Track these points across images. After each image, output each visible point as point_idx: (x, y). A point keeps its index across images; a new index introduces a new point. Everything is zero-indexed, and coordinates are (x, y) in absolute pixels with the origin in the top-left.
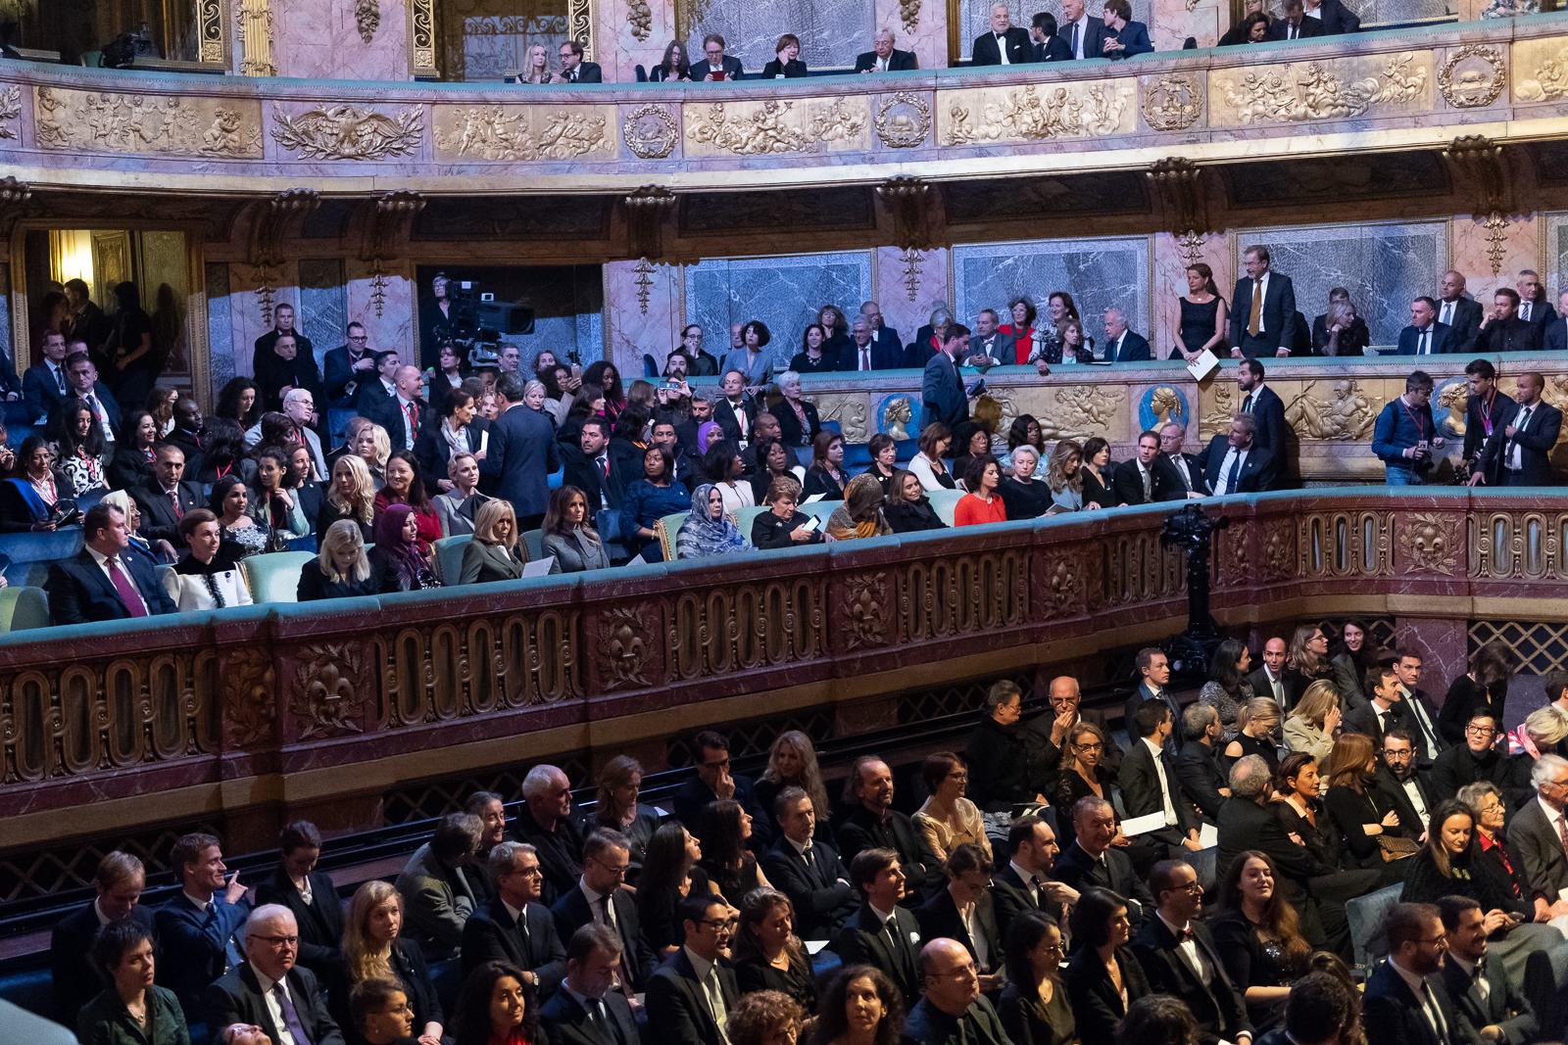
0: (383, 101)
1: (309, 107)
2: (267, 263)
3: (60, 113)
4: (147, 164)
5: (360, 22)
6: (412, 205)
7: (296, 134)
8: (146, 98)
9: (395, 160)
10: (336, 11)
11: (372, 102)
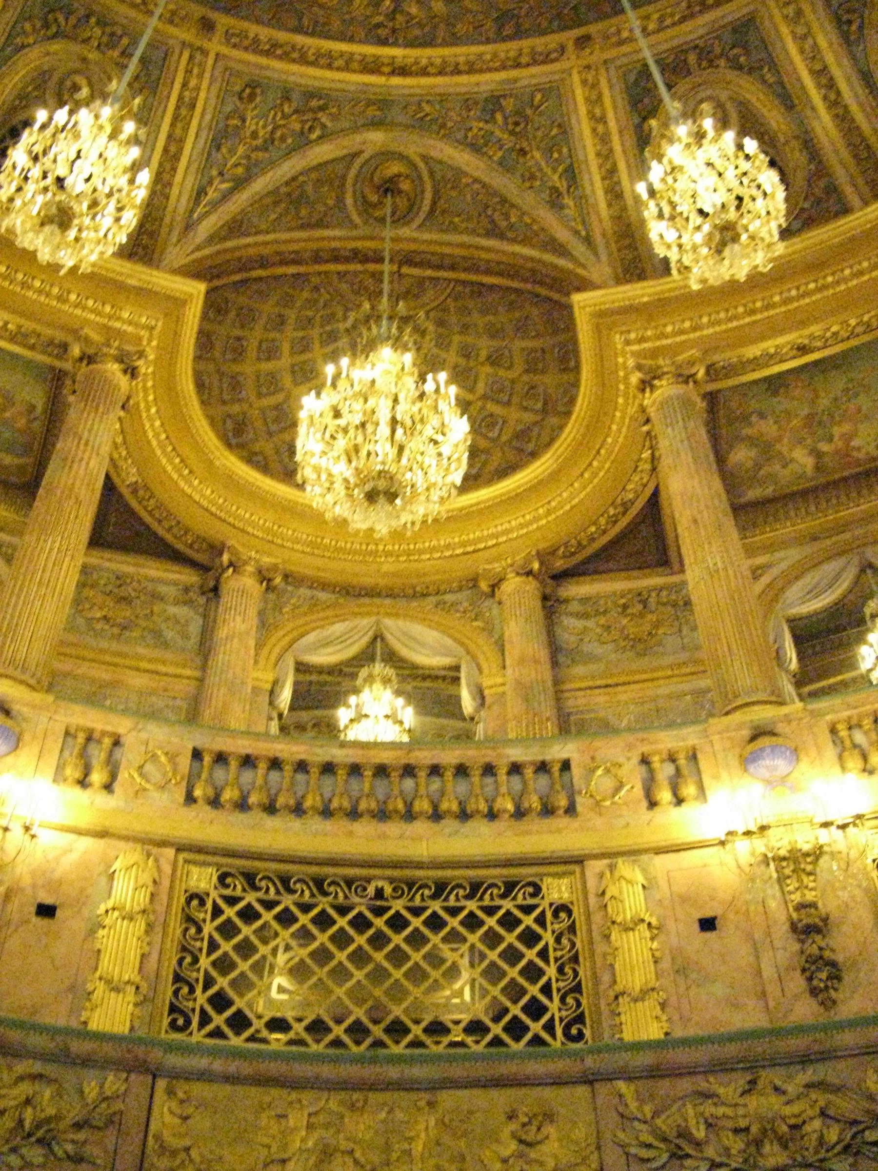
0: (826, 1056)
1: (685, 1085)
3: (201, 1123)
5: (810, 979)
7: (665, 1140)
8: (371, 1095)
11: (805, 1060)
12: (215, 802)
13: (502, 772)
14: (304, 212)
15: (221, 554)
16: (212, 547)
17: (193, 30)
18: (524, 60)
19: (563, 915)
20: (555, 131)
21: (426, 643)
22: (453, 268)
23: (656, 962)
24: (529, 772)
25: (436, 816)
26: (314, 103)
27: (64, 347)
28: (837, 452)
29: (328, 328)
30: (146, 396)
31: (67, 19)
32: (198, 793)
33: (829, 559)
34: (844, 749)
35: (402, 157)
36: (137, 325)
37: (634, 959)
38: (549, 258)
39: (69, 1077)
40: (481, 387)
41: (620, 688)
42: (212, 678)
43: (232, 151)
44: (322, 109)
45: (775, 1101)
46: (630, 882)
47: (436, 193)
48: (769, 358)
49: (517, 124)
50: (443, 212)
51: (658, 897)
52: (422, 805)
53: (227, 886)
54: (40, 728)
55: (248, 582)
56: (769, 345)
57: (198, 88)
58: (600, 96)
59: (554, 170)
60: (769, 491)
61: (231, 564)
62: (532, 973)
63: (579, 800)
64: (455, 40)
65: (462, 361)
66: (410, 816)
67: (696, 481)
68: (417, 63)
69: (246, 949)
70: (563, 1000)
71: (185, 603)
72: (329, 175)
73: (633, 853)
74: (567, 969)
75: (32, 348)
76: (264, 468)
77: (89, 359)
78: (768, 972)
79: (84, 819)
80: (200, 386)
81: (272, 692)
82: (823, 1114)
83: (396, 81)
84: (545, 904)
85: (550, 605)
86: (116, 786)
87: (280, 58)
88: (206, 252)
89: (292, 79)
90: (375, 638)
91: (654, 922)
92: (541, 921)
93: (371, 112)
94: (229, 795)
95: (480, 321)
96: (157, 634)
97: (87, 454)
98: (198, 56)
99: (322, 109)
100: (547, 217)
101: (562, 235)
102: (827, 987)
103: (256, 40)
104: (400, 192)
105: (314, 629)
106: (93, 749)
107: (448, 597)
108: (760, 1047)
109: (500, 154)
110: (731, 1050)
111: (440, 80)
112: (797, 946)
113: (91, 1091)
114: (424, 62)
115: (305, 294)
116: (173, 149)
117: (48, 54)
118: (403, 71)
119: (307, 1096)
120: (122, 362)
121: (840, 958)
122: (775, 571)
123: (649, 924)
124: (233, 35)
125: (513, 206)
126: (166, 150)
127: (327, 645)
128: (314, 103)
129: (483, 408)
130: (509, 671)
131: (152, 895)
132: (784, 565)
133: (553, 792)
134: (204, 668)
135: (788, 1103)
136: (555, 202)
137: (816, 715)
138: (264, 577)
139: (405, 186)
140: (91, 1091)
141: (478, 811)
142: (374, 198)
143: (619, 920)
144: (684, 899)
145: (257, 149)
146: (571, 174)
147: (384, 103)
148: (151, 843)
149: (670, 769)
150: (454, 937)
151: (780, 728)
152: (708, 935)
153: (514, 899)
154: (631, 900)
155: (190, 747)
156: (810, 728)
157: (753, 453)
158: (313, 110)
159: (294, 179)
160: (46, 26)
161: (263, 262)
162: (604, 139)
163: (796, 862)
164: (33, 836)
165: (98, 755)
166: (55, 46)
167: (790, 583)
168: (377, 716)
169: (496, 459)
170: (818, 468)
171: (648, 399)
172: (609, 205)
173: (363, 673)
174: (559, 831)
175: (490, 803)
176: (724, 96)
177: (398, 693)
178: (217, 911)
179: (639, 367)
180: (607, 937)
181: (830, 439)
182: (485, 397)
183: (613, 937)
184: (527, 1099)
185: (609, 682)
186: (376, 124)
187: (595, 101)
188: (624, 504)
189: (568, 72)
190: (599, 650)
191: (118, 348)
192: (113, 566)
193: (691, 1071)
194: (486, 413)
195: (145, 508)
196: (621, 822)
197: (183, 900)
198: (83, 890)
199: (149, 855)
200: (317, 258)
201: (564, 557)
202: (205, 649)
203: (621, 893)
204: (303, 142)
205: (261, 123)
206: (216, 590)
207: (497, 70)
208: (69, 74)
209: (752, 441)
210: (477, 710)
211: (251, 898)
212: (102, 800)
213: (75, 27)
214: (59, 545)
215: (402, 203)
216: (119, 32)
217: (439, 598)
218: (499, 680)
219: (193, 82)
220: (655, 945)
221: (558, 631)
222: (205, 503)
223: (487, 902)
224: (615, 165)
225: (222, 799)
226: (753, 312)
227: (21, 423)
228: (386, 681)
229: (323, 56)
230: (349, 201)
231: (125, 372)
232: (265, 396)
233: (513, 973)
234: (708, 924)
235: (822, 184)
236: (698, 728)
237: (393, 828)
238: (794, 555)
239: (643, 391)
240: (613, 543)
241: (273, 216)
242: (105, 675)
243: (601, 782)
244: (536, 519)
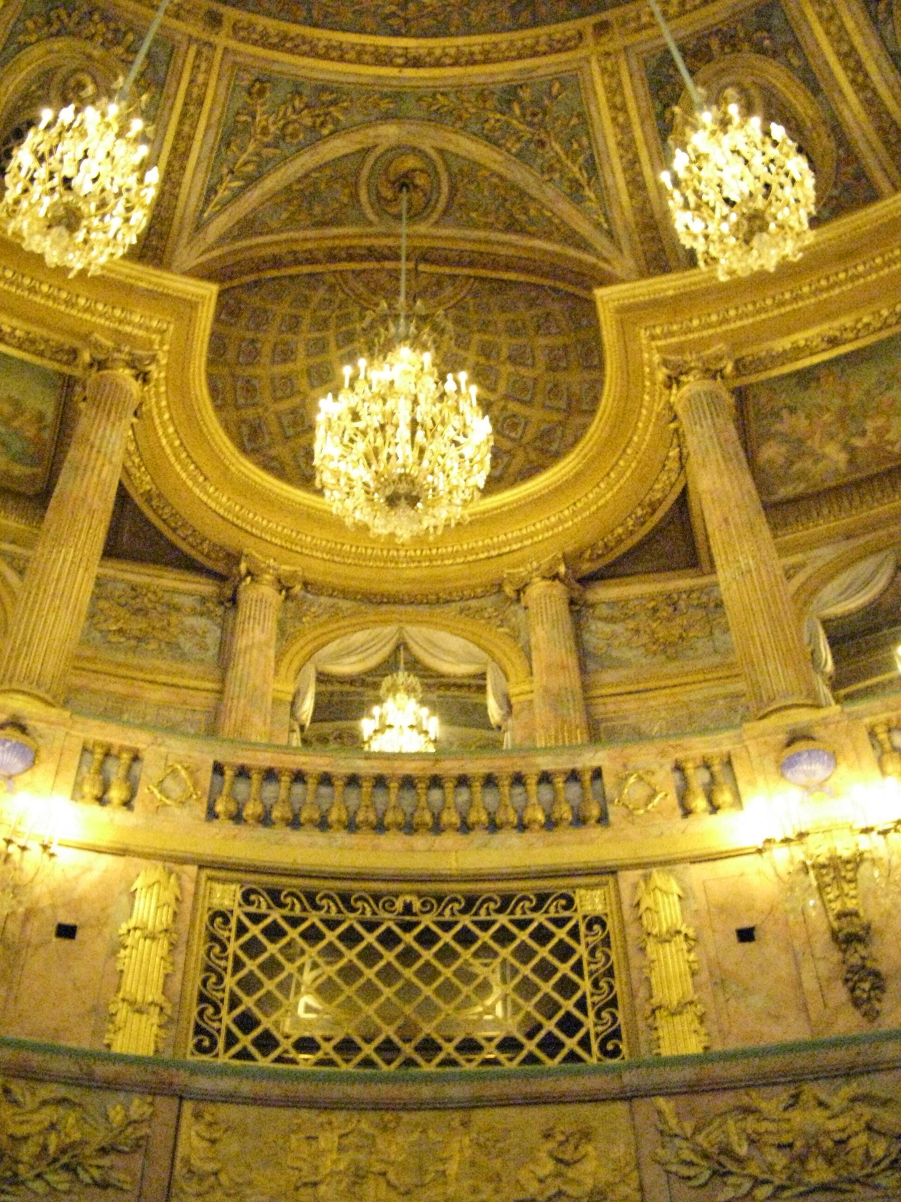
0: (871, 1069)
1: (725, 1101)
3: (231, 1146)
5: (852, 990)
7: (706, 1156)
8: (405, 1116)
10: (810, 983)
11: (849, 1073)
12: (237, 818)
13: (532, 781)
14: (317, 210)
15: (238, 563)
16: (229, 555)
17: (201, 24)
18: (542, 48)
19: (597, 927)
20: (574, 121)
21: (450, 650)
22: (471, 264)
23: (693, 974)
24: (559, 782)
25: (465, 827)
26: (326, 97)
27: (74, 353)
28: (872, 447)
29: (344, 328)
30: (158, 399)
31: (69, 15)
32: (219, 808)
33: (861, 558)
34: (883, 752)
35: (415, 151)
36: (148, 329)
37: (671, 971)
38: (572, 252)
39: (92, 1099)
40: (502, 387)
41: (650, 694)
42: (232, 689)
43: (243, 149)
44: (334, 103)
45: (819, 1115)
46: (666, 893)
47: (453, 189)
48: (797, 352)
49: (534, 115)
50: (461, 206)
51: (694, 907)
52: (450, 817)
53: (249, 903)
54: (57, 744)
55: (267, 591)
56: (800, 338)
57: (206, 84)
58: (620, 84)
59: (574, 162)
60: (801, 487)
61: (249, 573)
62: (566, 987)
63: (611, 809)
64: (469, 30)
65: (482, 360)
66: (437, 828)
67: (726, 479)
68: (430, 54)
69: (272, 967)
70: (598, 1015)
71: (202, 614)
72: (343, 172)
73: (667, 863)
74: (602, 984)
75: (41, 354)
76: (280, 473)
77: (100, 365)
78: (810, 983)
79: (105, 839)
80: (214, 391)
81: (293, 704)
82: (869, 1128)
83: (409, 72)
84: (577, 917)
85: (577, 608)
86: (136, 803)
87: (291, 51)
88: (216, 253)
89: (303, 72)
90: (398, 648)
91: (691, 933)
92: (574, 933)
93: (385, 105)
94: (252, 809)
95: (500, 319)
96: (173, 645)
97: (99, 463)
99: (334, 103)
100: (565, 209)
101: (584, 228)
102: (869, 999)
103: (265, 34)
104: (416, 187)
105: (333, 639)
106: (111, 765)
107: (473, 603)
108: (800, 1061)
109: (518, 146)
110: (772, 1063)
111: (457, 71)
112: (837, 956)
113: (117, 1115)
114: (438, 52)
115: (321, 293)
116: (182, 148)
117: (50, 52)
118: (416, 62)
119: (338, 1117)
120: (134, 367)
121: (883, 967)
122: (809, 570)
123: (686, 935)
124: (243, 28)
125: (533, 199)
126: (174, 149)
127: (349, 654)
128: (326, 97)
129: (504, 408)
130: (536, 678)
131: (175, 913)
132: (819, 563)
133: (584, 801)
134: (223, 680)
135: (830, 1118)
136: (575, 194)
137: (856, 718)
138: (283, 585)
139: (420, 180)
140: (117, 1115)
141: (508, 823)
142: (388, 194)
143: (655, 931)
144: (722, 909)
145: (267, 146)
146: (592, 167)
147: (397, 96)
148: (173, 860)
149: (704, 776)
150: (485, 952)
151: (819, 732)
152: (747, 946)
153: (546, 912)
154: (667, 908)
155: (211, 762)
156: (848, 732)
157: (783, 450)
158: (324, 105)
159: (306, 176)
161: (276, 262)
162: (625, 128)
163: (836, 869)
164: (52, 855)
165: (116, 770)
166: (57, 44)
167: (825, 582)
168: (401, 727)
169: (519, 460)
170: (851, 462)
171: (675, 396)
172: (631, 197)
173: (387, 682)
174: (592, 841)
175: (520, 813)
176: (747, 82)
177: (423, 702)
178: (242, 929)
179: (665, 363)
180: (643, 950)
181: (864, 433)
182: (506, 397)
183: (649, 949)
185: (641, 686)
186: (387, 117)
187: (614, 90)
188: (651, 504)
189: (587, 60)
190: (629, 654)
191: (130, 354)
192: (129, 576)
194: (506, 414)
195: (160, 516)
196: (655, 831)
197: (206, 918)
198: (103, 910)
199: (170, 873)
200: (332, 257)
201: (591, 560)
202: (224, 659)
203: (656, 904)
204: (315, 137)
205: (272, 119)
206: (234, 600)
207: (514, 59)
208: (75, 71)
209: (785, 438)
211: (276, 915)
212: (121, 816)
213: (78, 23)
214: (72, 557)
215: (418, 198)
216: (123, 28)
217: (461, 604)
218: (526, 687)
219: (201, 78)
220: (692, 957)
221: (586, 636)
222: (221, 512)
223: (518, 915)
224: (636, 155)
225: (244, 814)
226: (783, 304)
227: (30, 432)
228: (410, 690)
229: (334, 48)
230: (363, 196)
231: (137, 377)
232: (281, 399)
233: (547, 988)
234: (746, 935)
235: (850, 170)
236: (731, 733)
237: (420, 841)
238: (827, 554)
239: (670, 387)
240: (640, 546)
241: (285, 215)
242: (119, 687)
243: (634, 791)
244: (561, 522)
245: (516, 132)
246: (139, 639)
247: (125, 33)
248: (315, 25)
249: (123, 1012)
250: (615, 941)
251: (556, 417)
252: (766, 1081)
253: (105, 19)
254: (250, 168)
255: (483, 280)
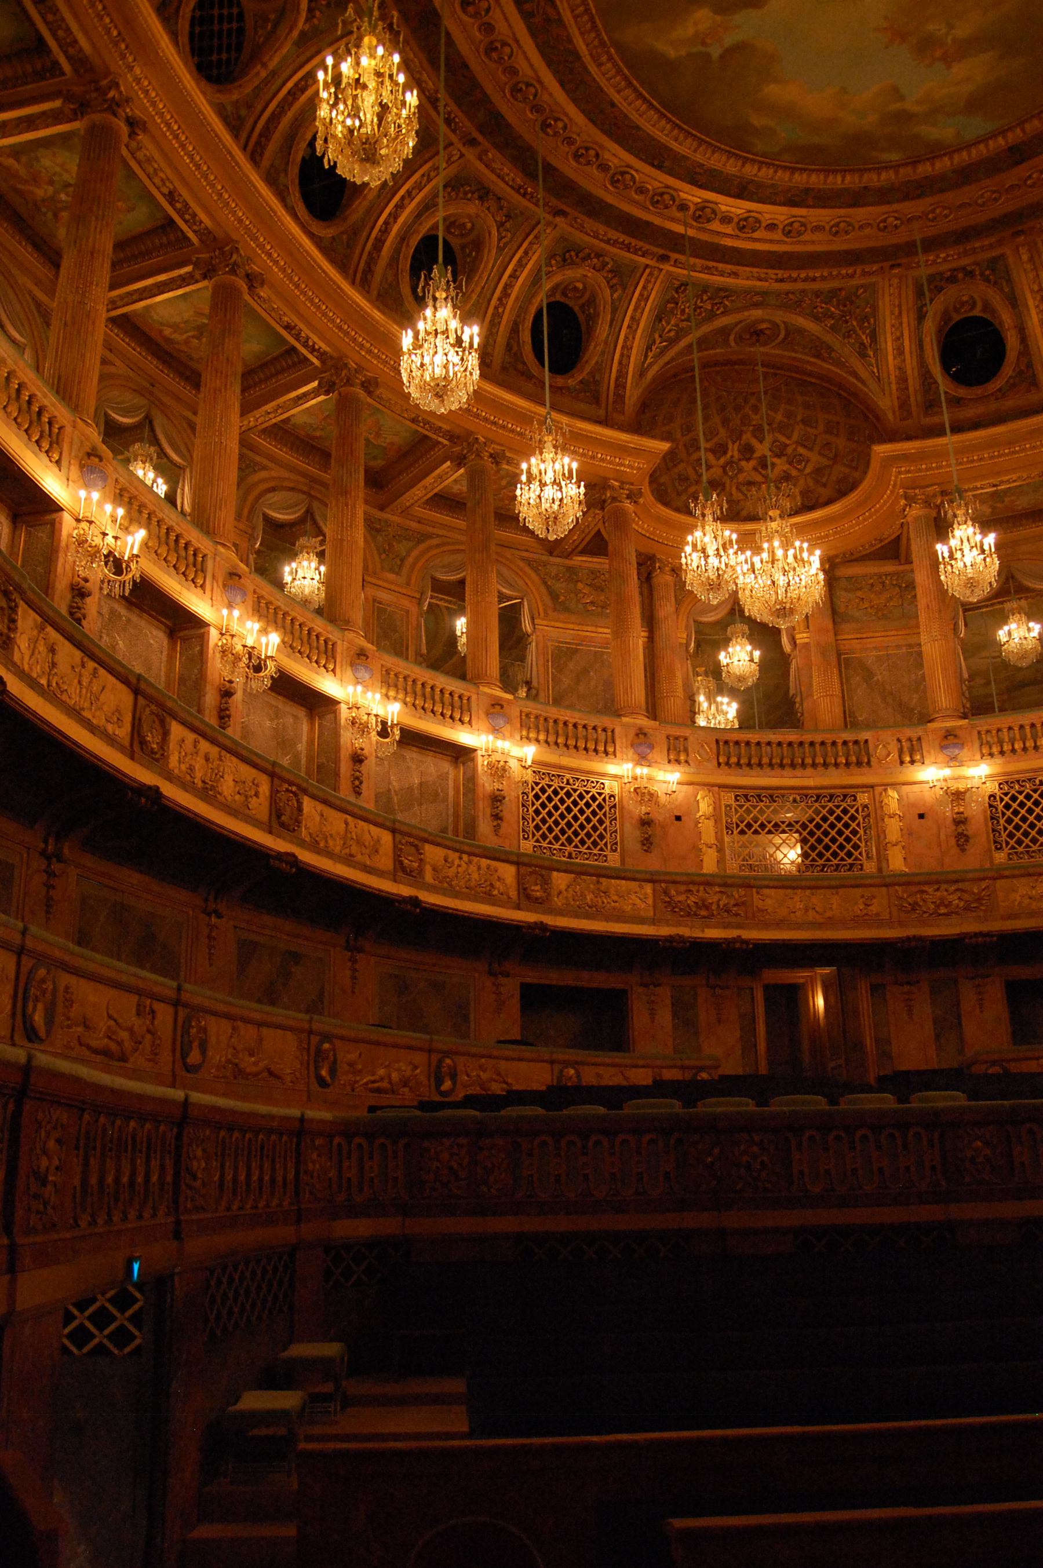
0: (963, 881)
2: (908, 983)
3: (769, 901)
4: (820, 926)
6: (988, 939)
9: (974, 914)
10: (943, 837)
11: (956, 881)
12: (727, 764)
26: (722, 294)
37: (893, 829)
40: (795, 437)
43: (668, 323)
44: (727, 297)
45: (945, 893)
59: (864, 333)
65: (785, 420)
72: (725, 331)
76: (677, 510)
78: (943, 837)
79: (686, 778)
92: (857, 811)
93: (756, 299)
94: (733, 760)
98: (656, 273)
99: (727, 297)
100: (855, 363)
101: (864, 374)
112: (954, 828)
121: (969, 833)
126: (629, 327)
128: (722, 294)
129: (795, 449)
133: (860, 757)
137: (973, 727)
139: (767, 332)
144: (913, 805)
145: (683, 321)
146: (873, 336)
151: (958, 732)
160: (564, 260)
172: (895, 358)
176: (976, 296)
182: (797, 443)
184: (868, 892)
185: (864, 636)
186: (756, 305)
193: (919, 883)
204: (712, 316)
210: (792, 651)
212: (687, 769)
216: (607, 259)
234: (921, 816)
245: (833, 313)
246: (603, 607)
247: (608, 263)
248: (726, 262)
249: (704, 848)
250: (873, 815)
251: (825, 462)
252: (929, 883)
253: (598, 256)
254: (672, 334)
255: (792, 377)
